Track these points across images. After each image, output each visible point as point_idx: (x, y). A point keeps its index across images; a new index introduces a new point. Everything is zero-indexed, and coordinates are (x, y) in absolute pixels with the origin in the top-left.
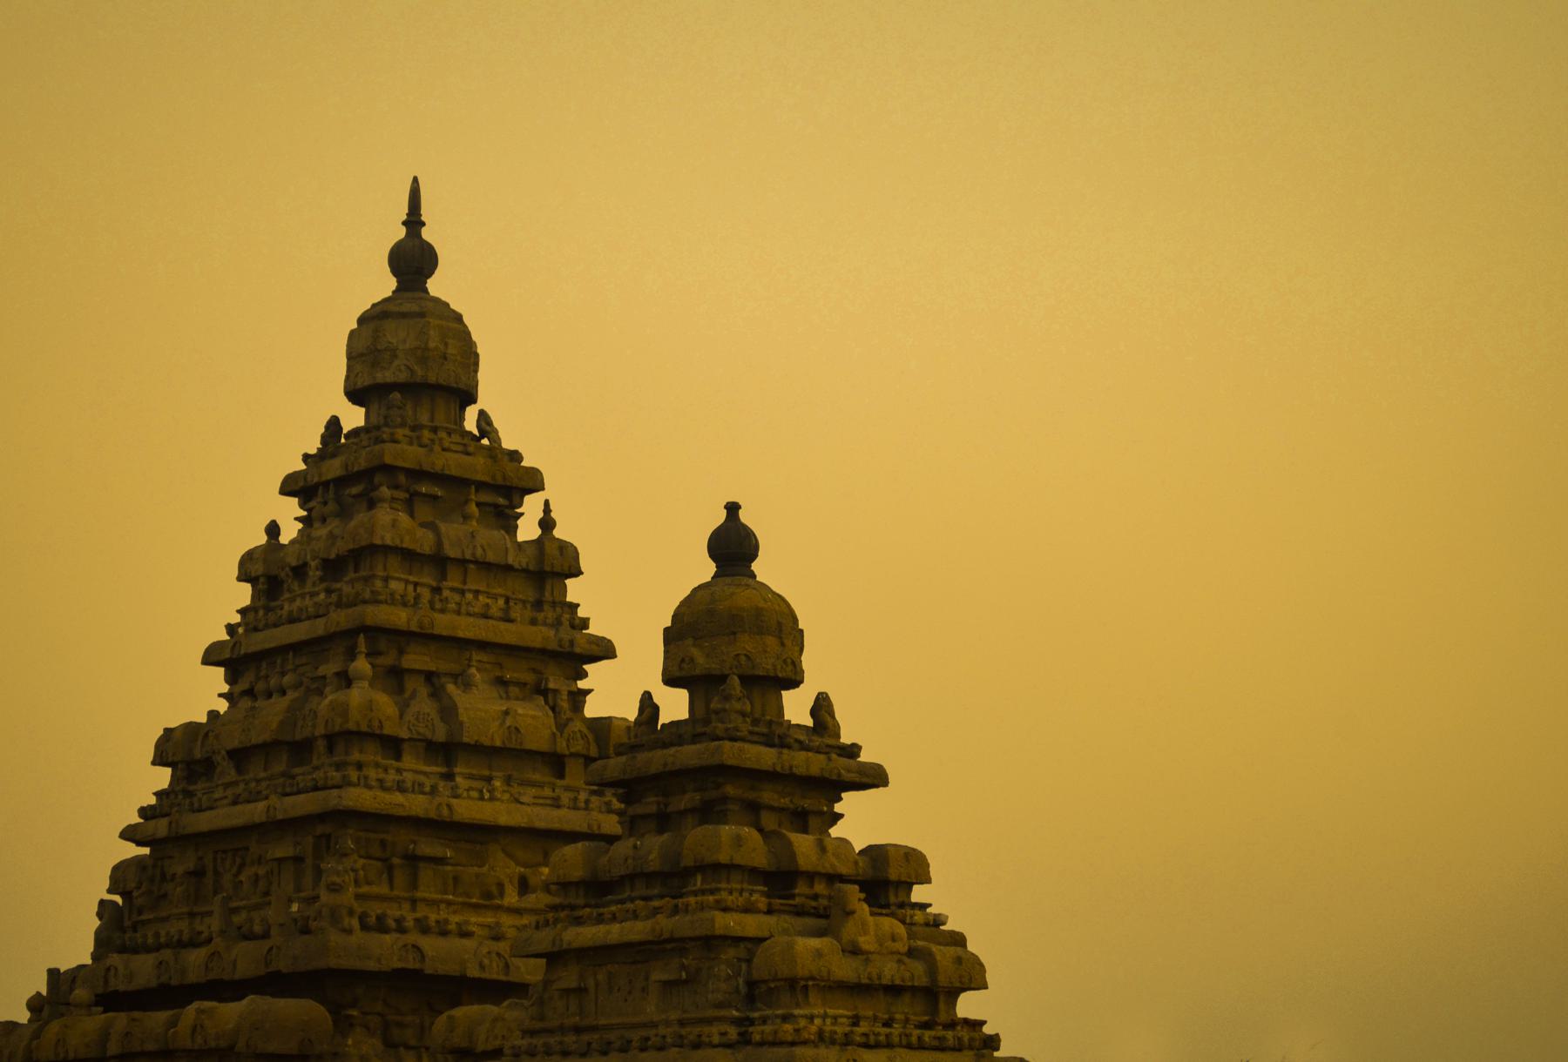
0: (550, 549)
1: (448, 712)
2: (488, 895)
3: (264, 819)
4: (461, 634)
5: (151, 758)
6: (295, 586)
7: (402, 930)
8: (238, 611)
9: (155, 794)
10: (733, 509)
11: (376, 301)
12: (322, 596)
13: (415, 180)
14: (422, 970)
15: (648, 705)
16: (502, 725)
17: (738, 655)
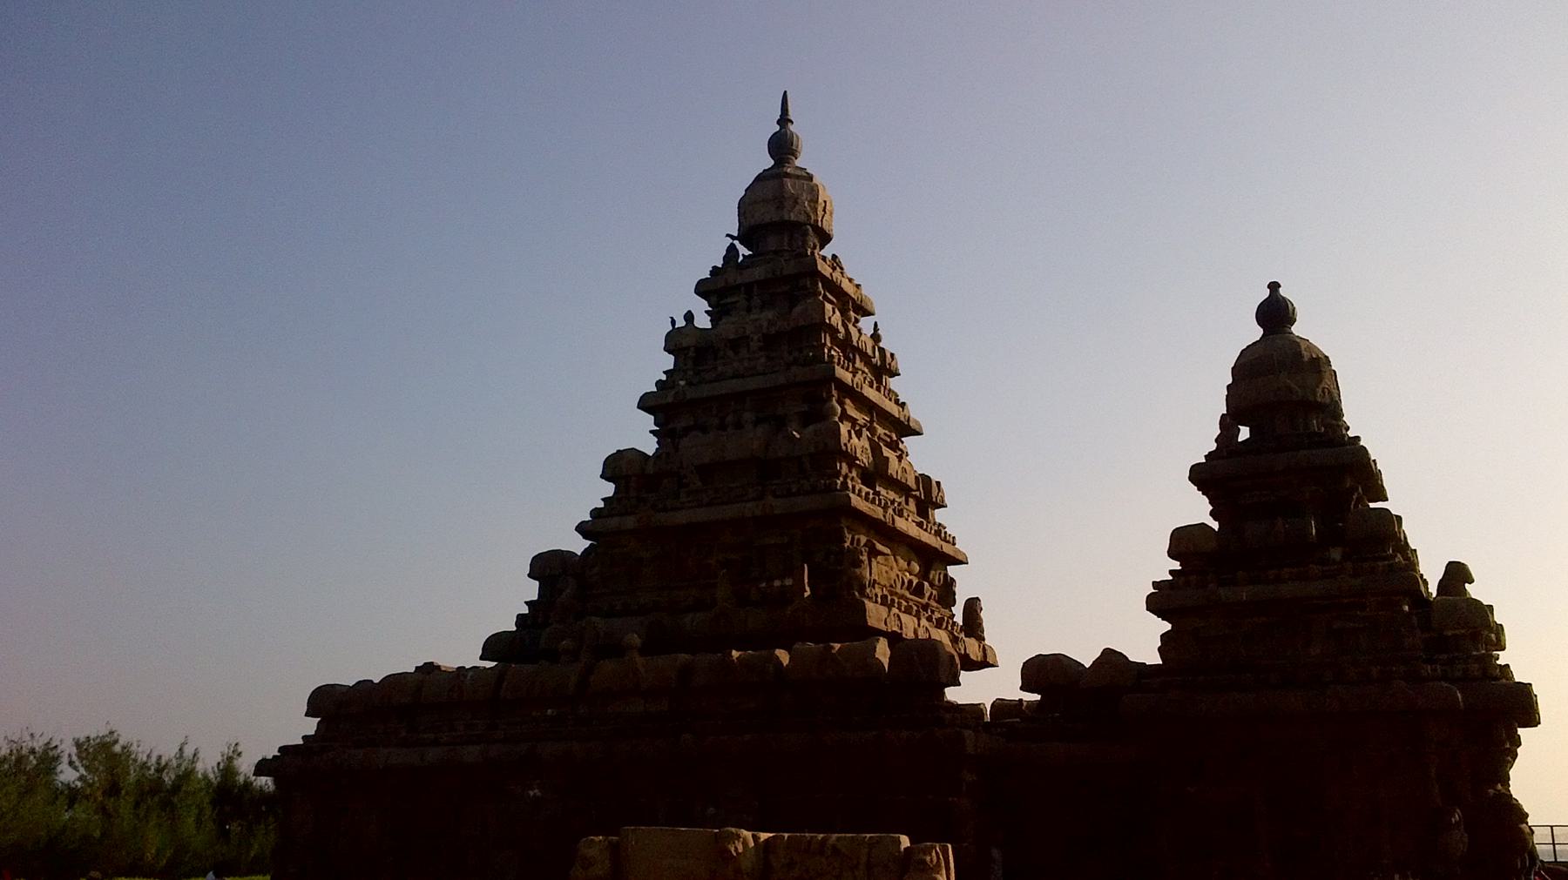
0: (888, 355)
1: (876, 449)
2: (891, 586)
3: (758, 513)
4: (871, 398)
5: (600, 473)
6: (730, 353)
7: (876, 602)
8: (664, 372)
9: (603, 499)
10: (1274, 287)
11: (767, 168)
12: (763, 360)
13: (785, 92)
14: (901, 634)
15: (1228, 425)
16: (900, 465)
17: (1324, 388)
